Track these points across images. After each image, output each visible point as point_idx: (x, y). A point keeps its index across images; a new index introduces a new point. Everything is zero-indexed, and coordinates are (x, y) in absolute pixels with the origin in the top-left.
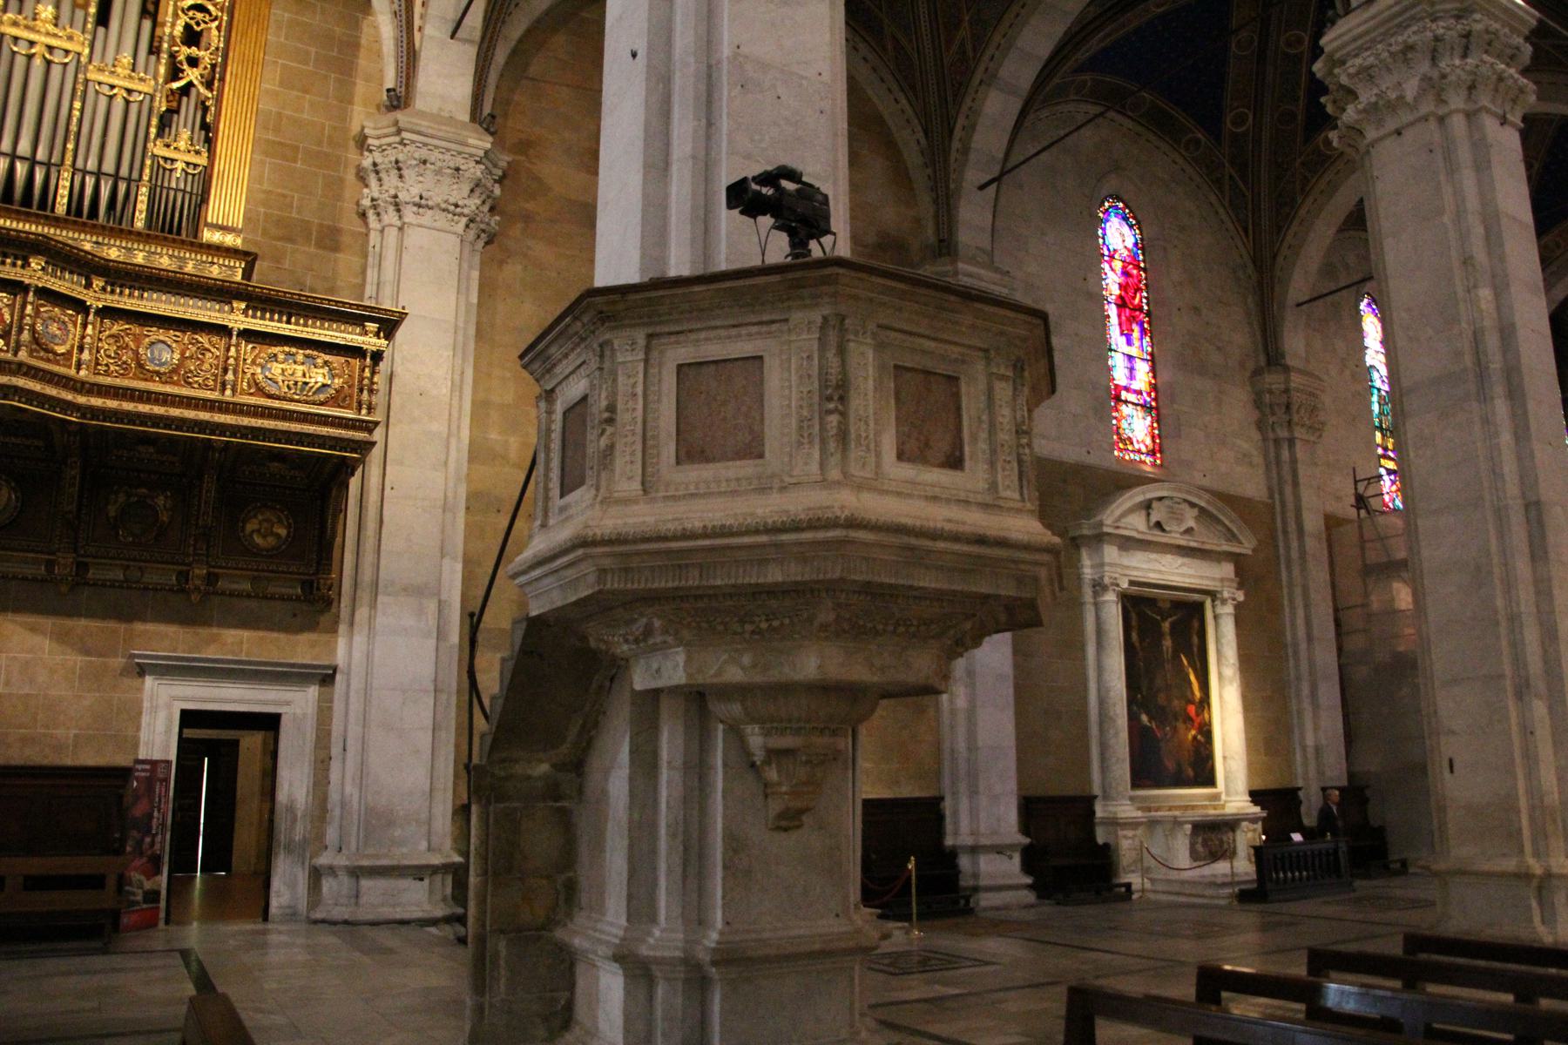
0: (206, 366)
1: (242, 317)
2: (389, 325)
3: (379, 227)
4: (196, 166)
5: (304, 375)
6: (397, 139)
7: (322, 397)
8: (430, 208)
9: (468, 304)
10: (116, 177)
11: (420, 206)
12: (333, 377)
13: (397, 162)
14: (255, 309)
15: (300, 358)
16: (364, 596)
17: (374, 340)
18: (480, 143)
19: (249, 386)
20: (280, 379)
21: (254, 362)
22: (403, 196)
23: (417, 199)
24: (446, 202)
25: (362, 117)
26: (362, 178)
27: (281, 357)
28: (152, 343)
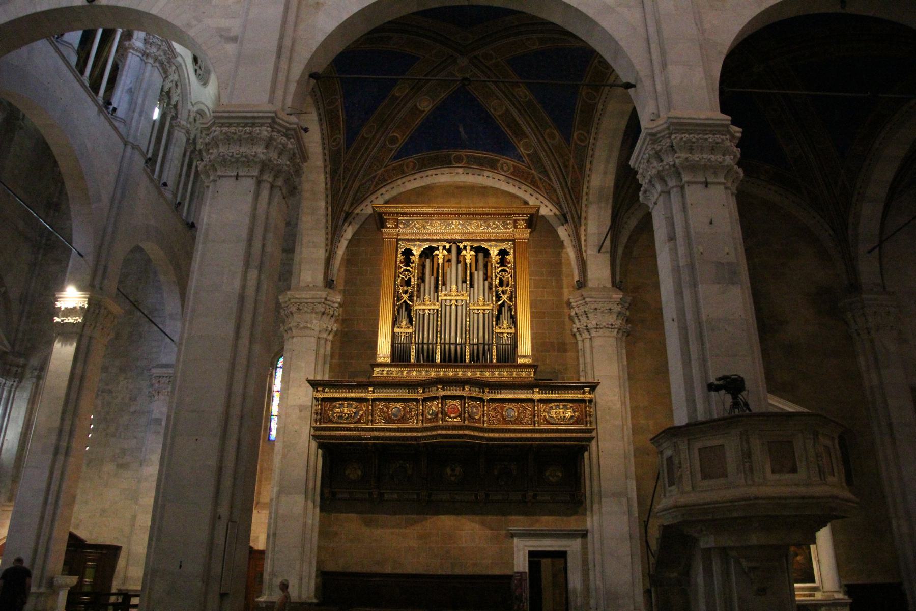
0: (527, 415)
1: (538, 395)
2: (593, 387)
3: (581, 339)
4: (511, 333)
5: (564, 413)
6: (584, 301)
7: (572, 421)
8: (601, 328)
9: (623, 365)
10: (484, 344)
11: (597, 328)
12: (574, 412)
13: (585, 311)
14: (542, 390)
15: (561, 407)
16: (596, 499)
17: (589, 395)
18: (617, 296)
19: (544, 421)
20: (555, 416)
21: (544, 411)
22: (589, 326)
24: (607, 324)
25: (567, 294)
26: (571, 319)
27: (554, 407)
28: (507, 410)
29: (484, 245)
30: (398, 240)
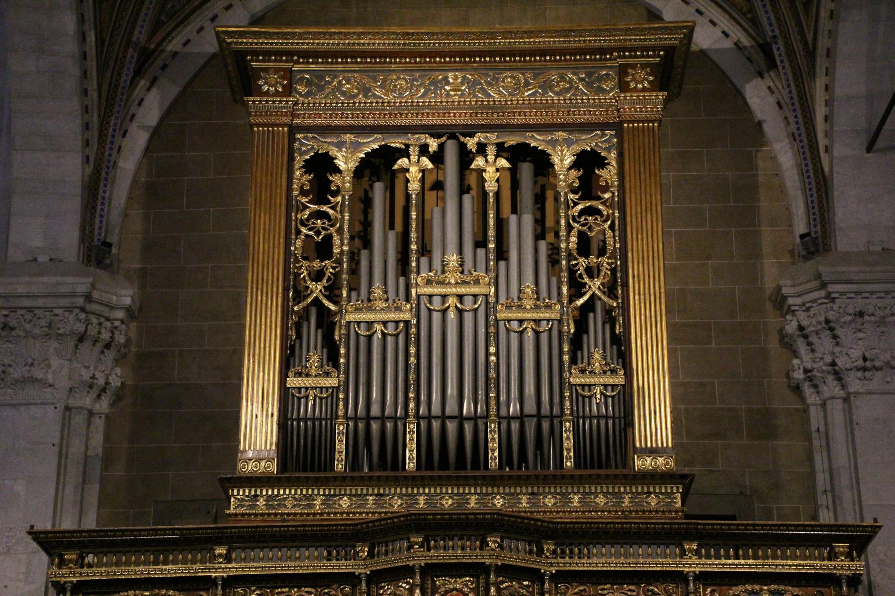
23: (860, 363)
29: (537, 141)
30: (293, 130)
